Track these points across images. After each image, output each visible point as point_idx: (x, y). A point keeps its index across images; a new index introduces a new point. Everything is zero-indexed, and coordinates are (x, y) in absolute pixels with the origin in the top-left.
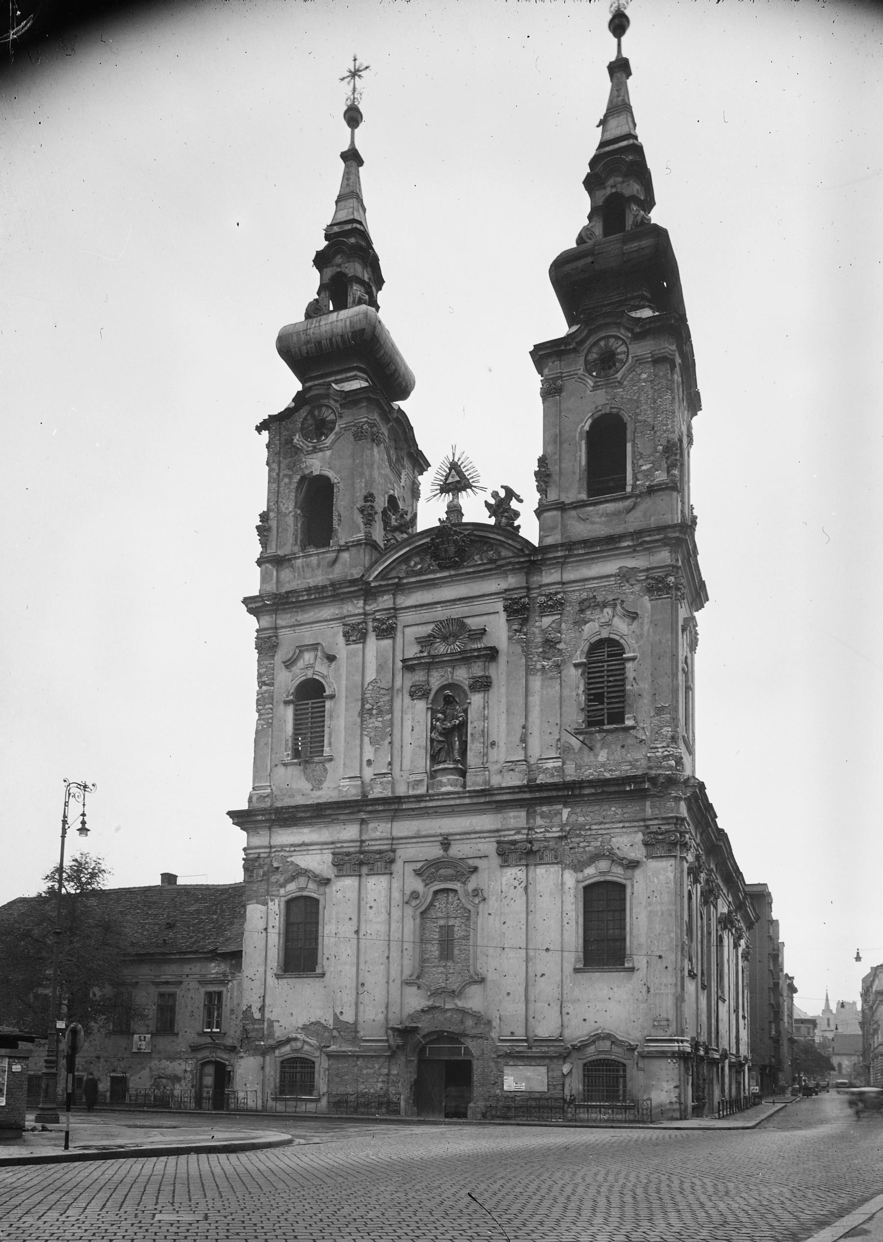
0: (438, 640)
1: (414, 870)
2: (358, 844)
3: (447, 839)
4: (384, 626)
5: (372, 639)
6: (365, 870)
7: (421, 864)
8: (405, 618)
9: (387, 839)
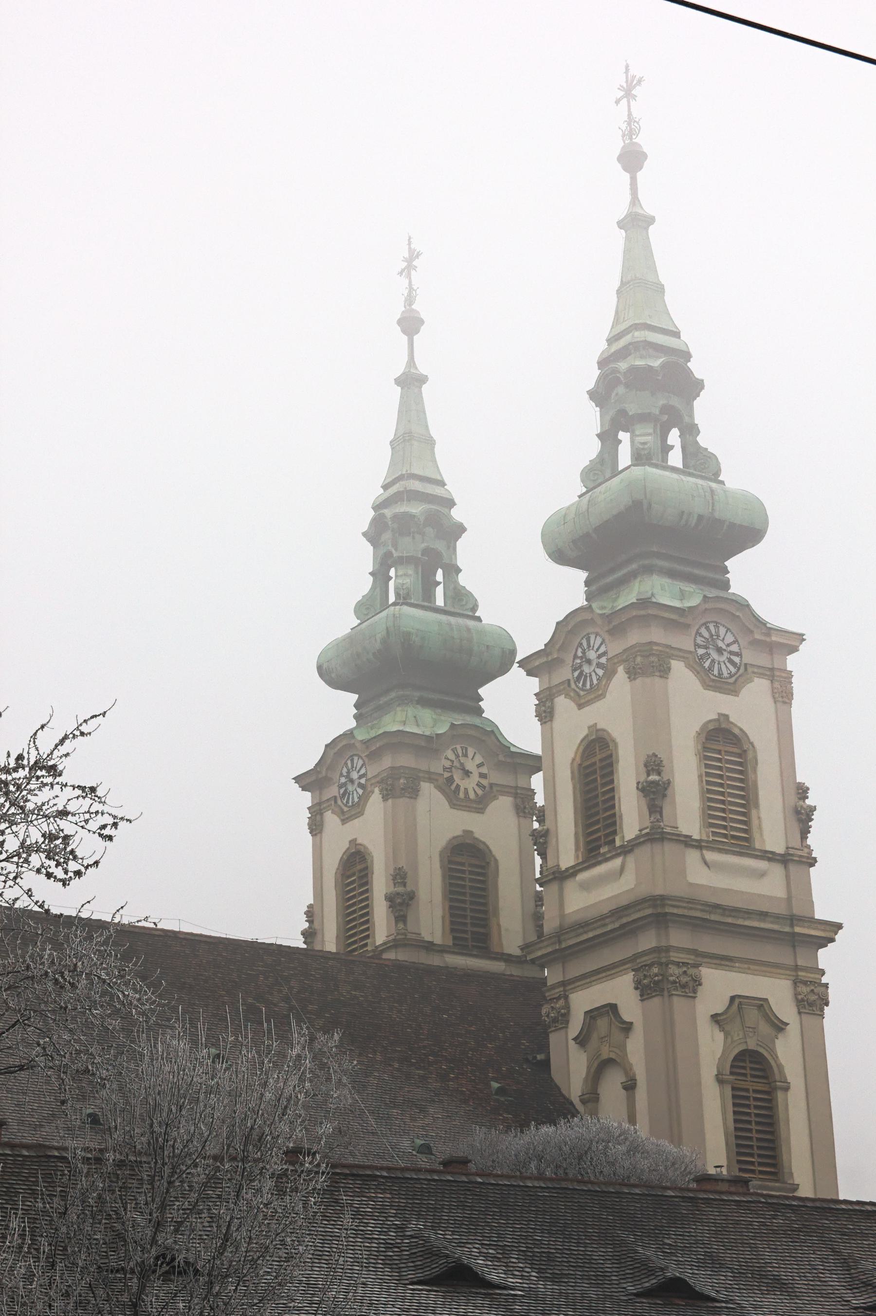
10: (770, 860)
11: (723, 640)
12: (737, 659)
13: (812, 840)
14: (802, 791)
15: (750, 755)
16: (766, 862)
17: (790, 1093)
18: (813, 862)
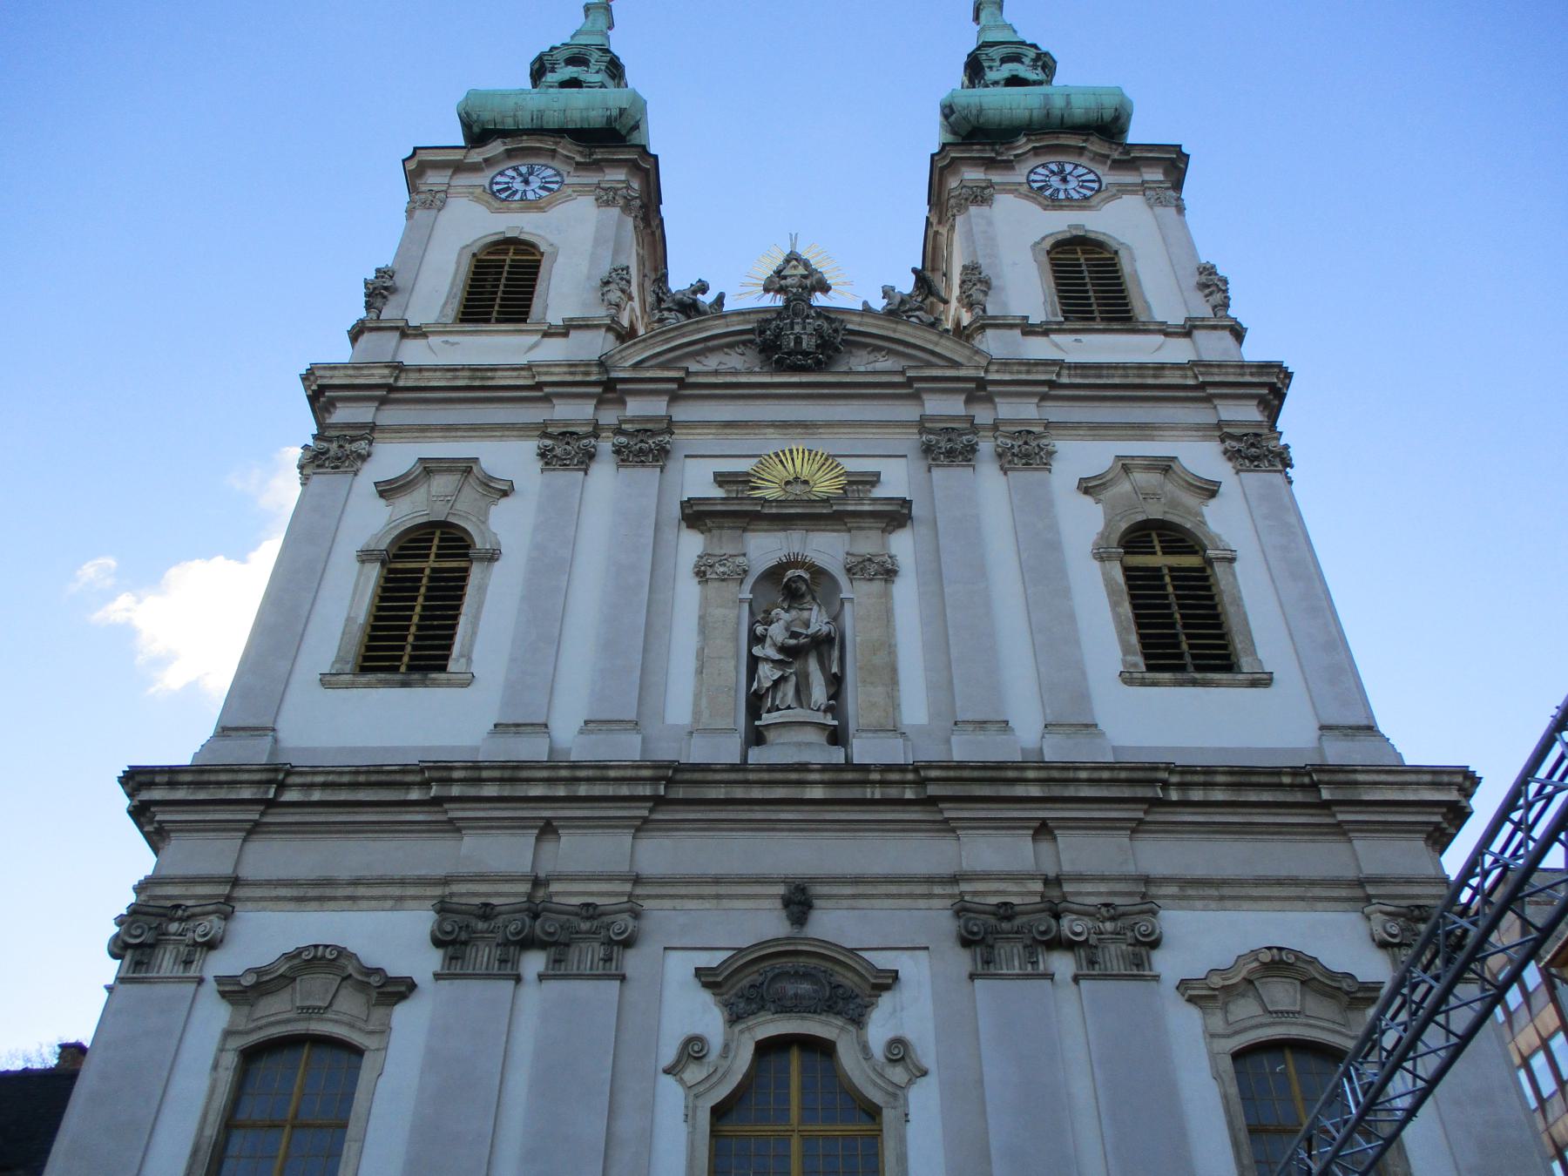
2: (525, 888)
5: (604, 473)
6: (533, 963)
7: (725, 955)
9: (610, 878)
10: (1167, 334)
12: (1096, 186)
14: (1208, 270)
16: (1163, 337)
17: (1236, 565)
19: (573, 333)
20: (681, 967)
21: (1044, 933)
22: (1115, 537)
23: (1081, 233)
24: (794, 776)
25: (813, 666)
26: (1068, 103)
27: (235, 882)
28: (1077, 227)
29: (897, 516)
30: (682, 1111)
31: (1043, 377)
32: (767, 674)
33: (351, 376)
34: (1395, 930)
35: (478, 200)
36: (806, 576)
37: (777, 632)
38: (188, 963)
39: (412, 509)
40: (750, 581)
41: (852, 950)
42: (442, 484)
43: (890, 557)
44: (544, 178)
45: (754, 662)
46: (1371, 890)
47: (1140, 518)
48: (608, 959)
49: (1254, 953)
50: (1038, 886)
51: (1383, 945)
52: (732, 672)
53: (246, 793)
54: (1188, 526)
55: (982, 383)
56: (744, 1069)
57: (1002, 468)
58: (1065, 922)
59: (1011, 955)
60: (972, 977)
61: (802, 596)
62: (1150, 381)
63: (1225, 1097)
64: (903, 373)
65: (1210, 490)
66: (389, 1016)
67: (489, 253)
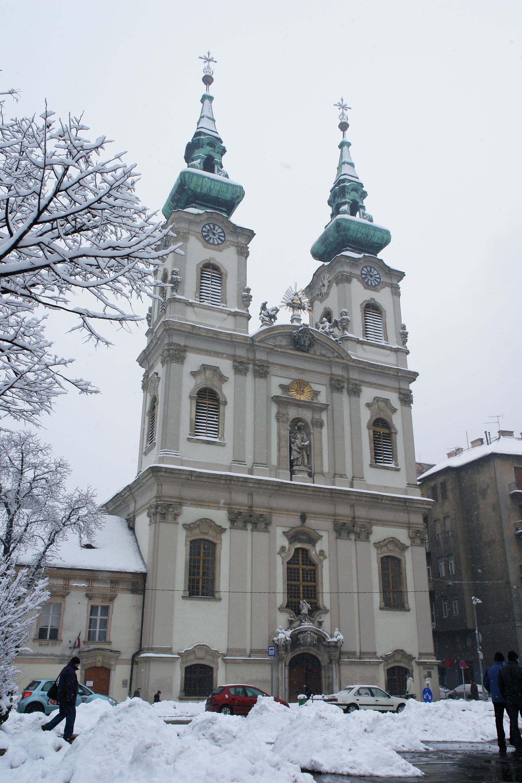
0: (294, 391)
1: (284, 533)
2: (247, 508)
3: (304, 515)
4: (262, 371)
5: (250, 377)
8: (273, 370)
9: (266, 508)
11: (373, 273)
12: (379, 280)
13: (407, 344)
14: (404, 327)
15: (383, 313)
17: (397, 435)
18: (408, 353)
19: (238, 317)
20: (279, 531)
21: (351, 530)
22: (372, 421)
23: (372, 302)
24: (306, 488)
25: (305, 453)
26: (374, 235)
27: (182, 499)
28: (373, 299)
29: (324, 408)
30: (281, 562)
31: (362, 366)
32: (295, 455)
33: (179, 326)
34: (413, 535)
35: (198, 239)
36: (303, 424)
37: (298, 441)
38: (175, 519)
39: (201, 382)
40: (289, 422)
41: (313, 530)
42: (208, 373)
43: (323, 421)
44: (219, 233)
45: (291, 448)
46: (411, 526)
47: (378, 417)
48: (266, 528)
49: (389, 538)
50: (350, 519)
51: (411, 538)
52: (285, 451)
53: (184, 477)
54: (389, 421)
55: (347, 365)
56: (293, 554)
57: (349, 394)
58: (355, 528)
59: (344, 534)
60: (337, 538)
61: (302, 430)
62: (387, 372)
63: (378, 567)
64: (329, 357)
65: (394, 410)
66: (221, 536)
67: (204, 267)
